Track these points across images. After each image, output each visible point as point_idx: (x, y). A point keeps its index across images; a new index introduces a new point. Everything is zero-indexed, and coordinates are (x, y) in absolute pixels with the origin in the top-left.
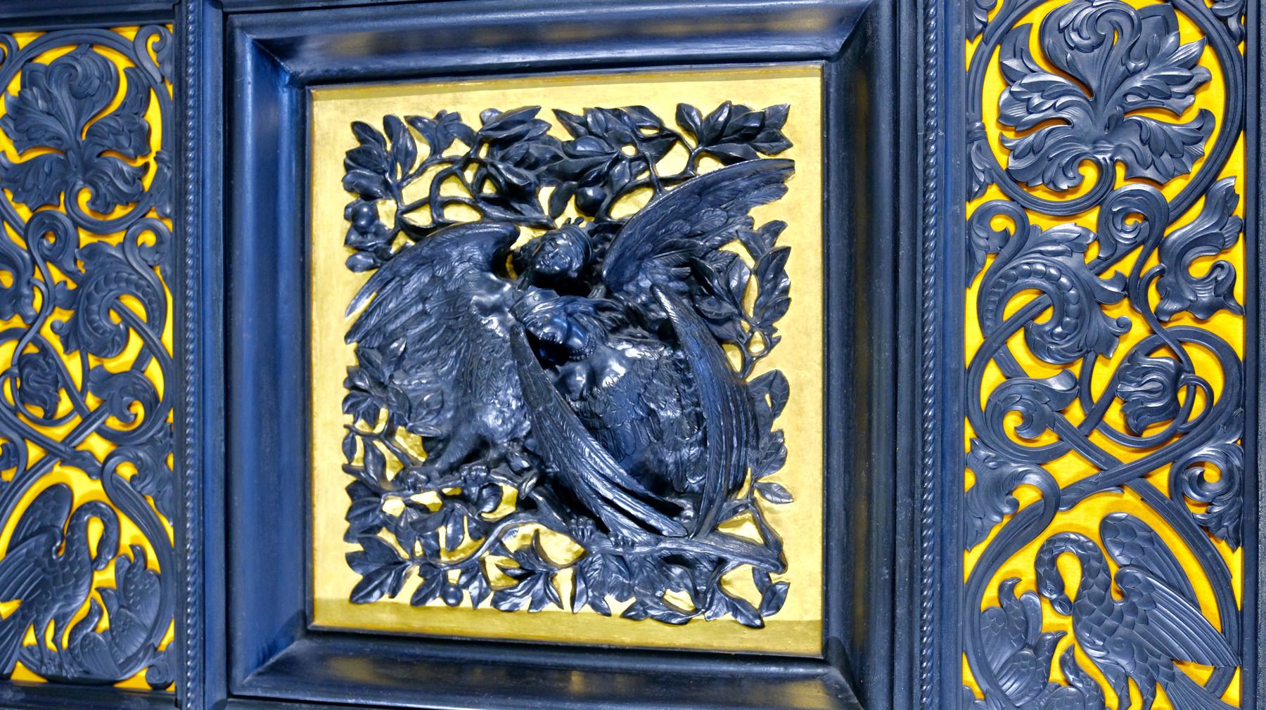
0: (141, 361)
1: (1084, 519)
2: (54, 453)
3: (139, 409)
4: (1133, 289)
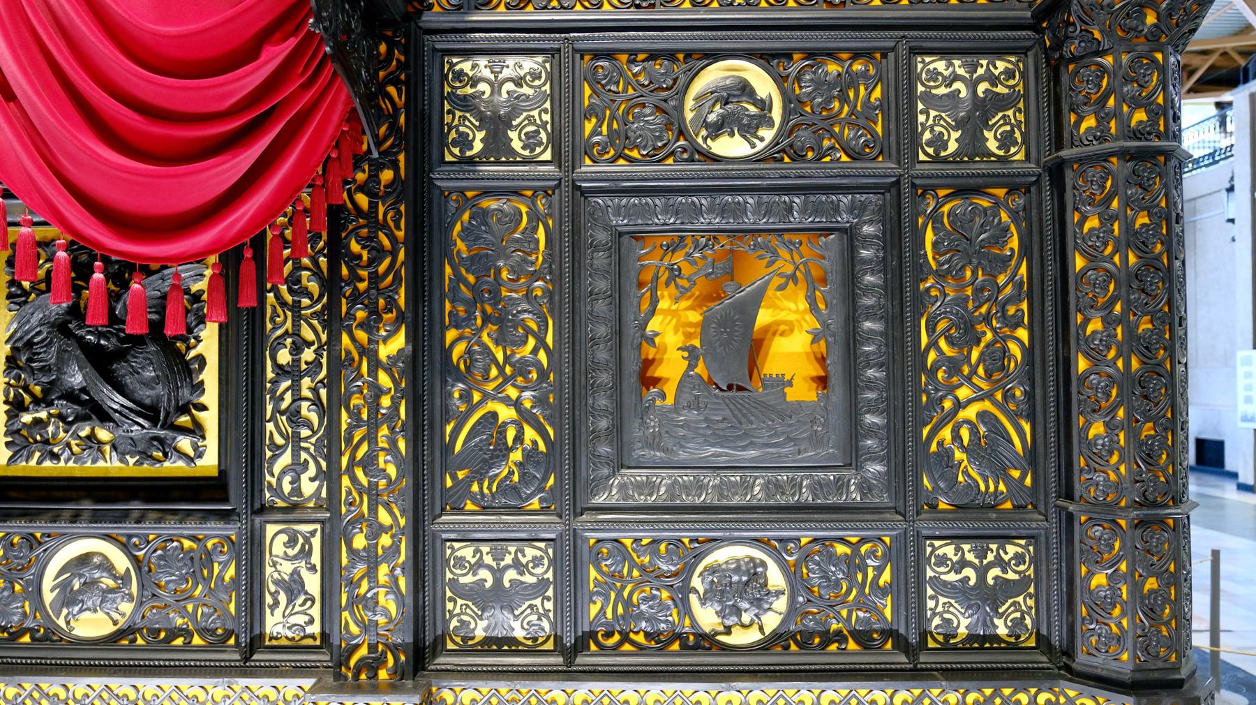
0: (535, 351)
1: (970, 413)
2: (486, 397)
3: (534, 375)
4: (987, 319)
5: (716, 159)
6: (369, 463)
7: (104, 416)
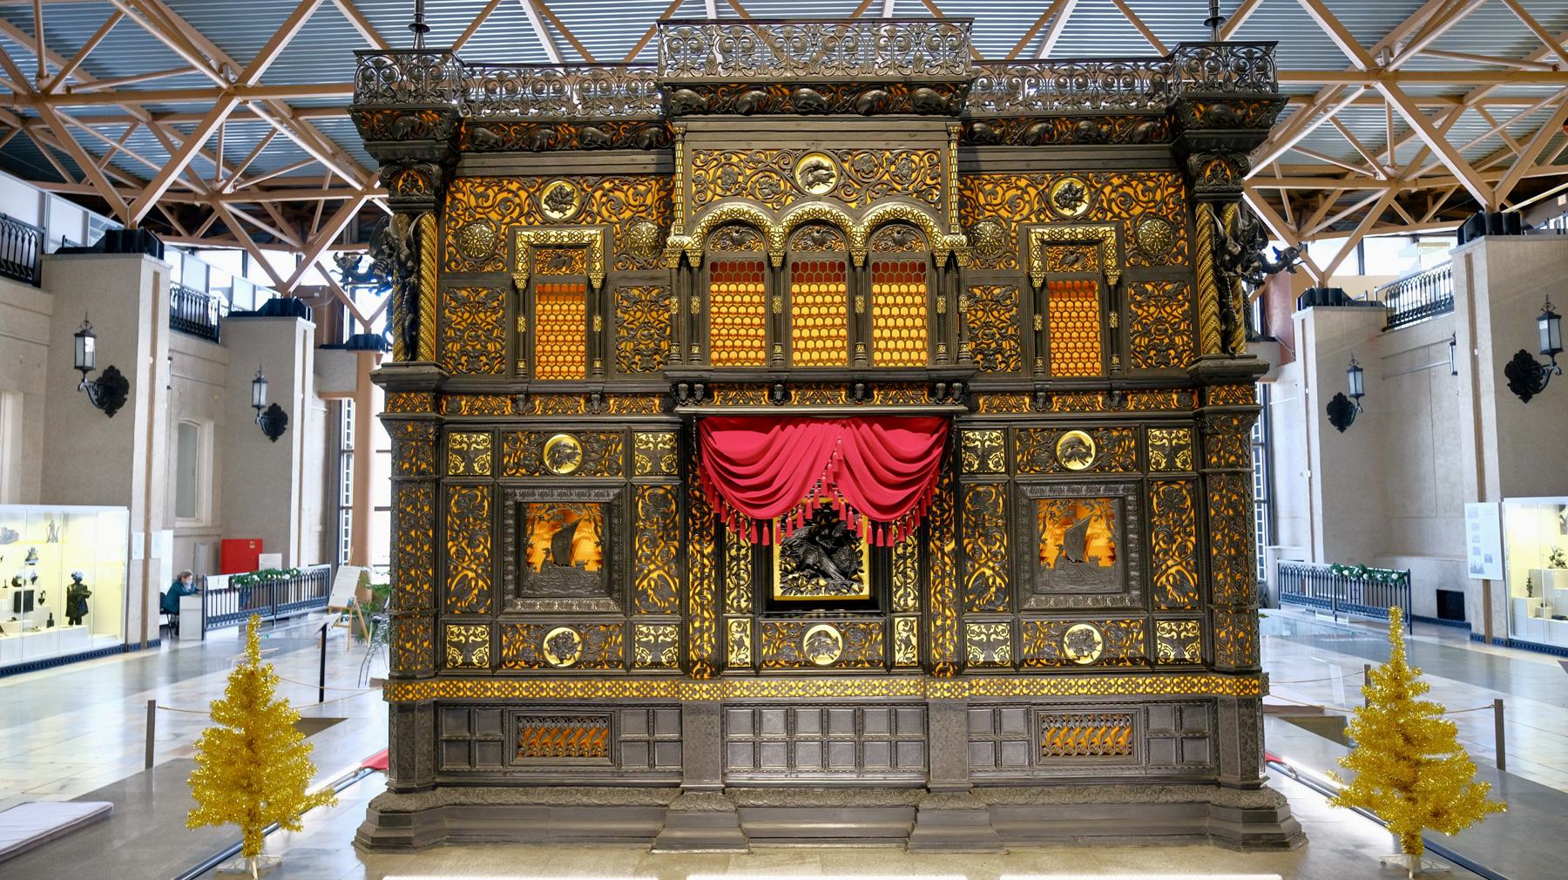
1: (1173, 570)
5: (1070, 471)
6: (942, 592)
7: (826, 575)
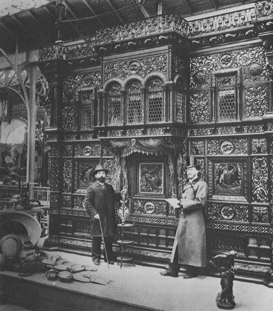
1: (259, 189)
